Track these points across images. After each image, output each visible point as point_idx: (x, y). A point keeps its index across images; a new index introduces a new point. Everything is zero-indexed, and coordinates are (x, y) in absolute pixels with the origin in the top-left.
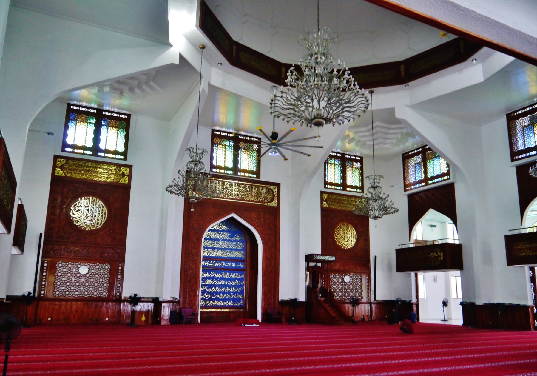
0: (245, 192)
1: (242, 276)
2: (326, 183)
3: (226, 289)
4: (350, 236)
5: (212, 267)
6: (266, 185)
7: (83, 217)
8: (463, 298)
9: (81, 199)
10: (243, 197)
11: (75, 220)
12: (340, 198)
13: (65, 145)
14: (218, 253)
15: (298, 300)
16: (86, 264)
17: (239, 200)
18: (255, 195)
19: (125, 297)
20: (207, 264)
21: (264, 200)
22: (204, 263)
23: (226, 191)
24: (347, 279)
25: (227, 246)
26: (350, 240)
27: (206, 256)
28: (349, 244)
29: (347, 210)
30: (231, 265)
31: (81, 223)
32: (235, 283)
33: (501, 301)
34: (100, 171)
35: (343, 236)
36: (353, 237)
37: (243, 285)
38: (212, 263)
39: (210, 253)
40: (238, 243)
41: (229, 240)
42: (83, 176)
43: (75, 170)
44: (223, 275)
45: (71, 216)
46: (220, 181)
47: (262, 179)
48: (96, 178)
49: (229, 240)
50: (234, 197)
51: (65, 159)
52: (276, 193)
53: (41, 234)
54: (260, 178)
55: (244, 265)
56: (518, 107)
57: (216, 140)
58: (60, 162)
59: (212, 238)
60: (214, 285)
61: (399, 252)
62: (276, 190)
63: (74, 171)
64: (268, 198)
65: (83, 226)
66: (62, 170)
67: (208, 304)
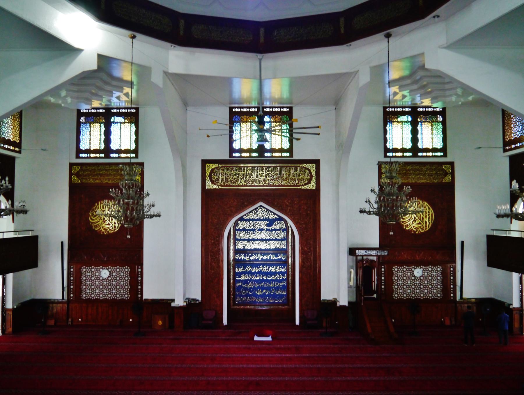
0: (274, 176)
1: (284, 269)
2: (387, 150)
3: (265, 284)
4: (424, 217)
5: (247, 261)
6: (301, 164)
7: (101, 221)
9: (98, 204)
10: (271, 182)
11: (94, 225)
12: (407, 168)
13: (79, 151)
14: (254, 245)
15: (338, 304)
16: (107, 268)
17: (267, 186)
18: (286, 178)
19: (145, 299)
20: (241, 258)
21: (299, 183)
22: (238, 256)
23: (250, 177)
24: (418, 272)
25: (264, 236)
27: (240, 249)
28: (422, 227)
29: (420, 183)
30: (270, 257)
31: (100, 227)
32: (275, 278)
34: (112, 173)
35: (413, 217)
36: (429, 218)
37: (285, 280)
38: (248, 256)
39: (244, 246)
40: (278, 232)
41: (267, 230)
42: (97, 181)
43: (88, 175)
44: (261, 269)
45: (90, 222)
46: (243, 167)
47: (296, 157)
48: (109, 181)
49: (267, 230)
50: (260, 183)
51: (79, 165)
52: (314, 173)
53: (62, 243)
54: (292, 157)
55: (286, 256)
57: (236, 118)
58: (75, 169)
59: (247, 228)
60: (251, 280)
62: (314, 168)
63: (89, 176)
64: (303, 179)
65: (101, 231)
66: (77, 177)
67: (245, 300)
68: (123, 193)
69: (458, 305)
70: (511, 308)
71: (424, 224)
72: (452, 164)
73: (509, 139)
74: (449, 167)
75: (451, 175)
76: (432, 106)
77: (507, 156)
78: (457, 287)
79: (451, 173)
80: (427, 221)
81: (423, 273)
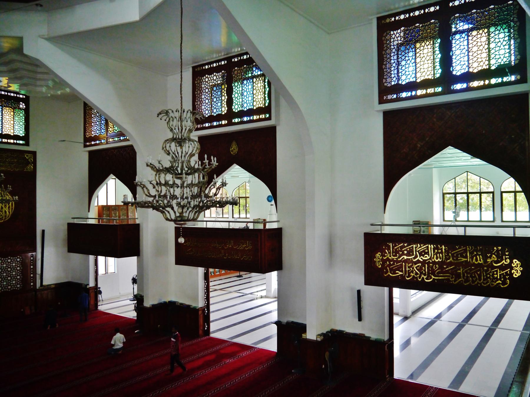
8: (137, 292)
26: (4, 211)
33: (174, 299)
36: (9, 207)
56: (213, 58)
61: (71, 227)
68: (137, 185)
69: (38, 293)
70: (88, 288)
71: (3, 213)
72: (34, 153)
73: (89, 136)
74: (31, 156)
75: (33, 165)
76: (21, 92)
77: (87, 151)
78: (37, 276)
79: (33, 163)
80: (7, 211)
81: (1, 265)
